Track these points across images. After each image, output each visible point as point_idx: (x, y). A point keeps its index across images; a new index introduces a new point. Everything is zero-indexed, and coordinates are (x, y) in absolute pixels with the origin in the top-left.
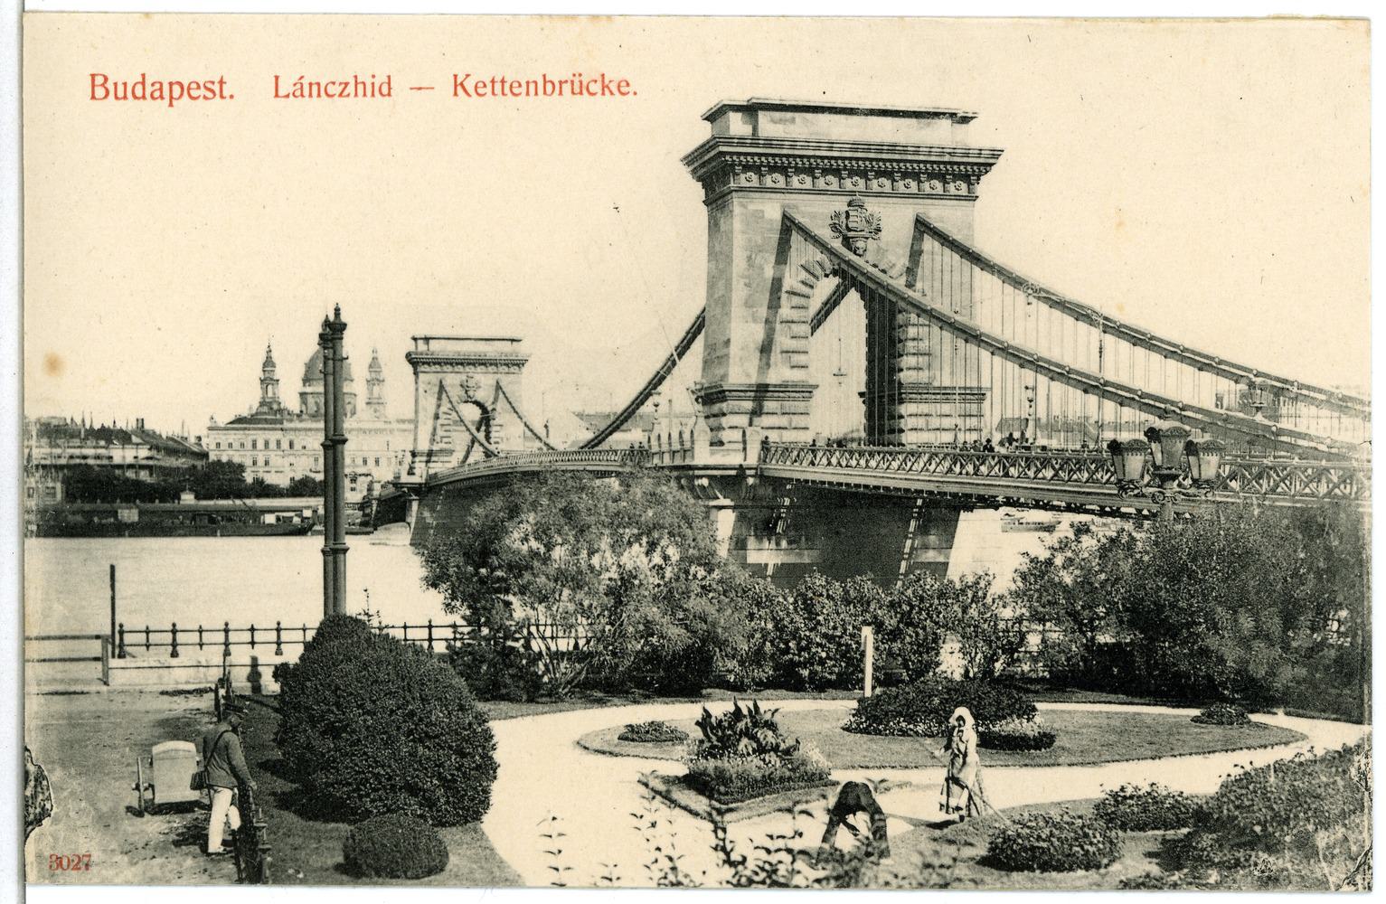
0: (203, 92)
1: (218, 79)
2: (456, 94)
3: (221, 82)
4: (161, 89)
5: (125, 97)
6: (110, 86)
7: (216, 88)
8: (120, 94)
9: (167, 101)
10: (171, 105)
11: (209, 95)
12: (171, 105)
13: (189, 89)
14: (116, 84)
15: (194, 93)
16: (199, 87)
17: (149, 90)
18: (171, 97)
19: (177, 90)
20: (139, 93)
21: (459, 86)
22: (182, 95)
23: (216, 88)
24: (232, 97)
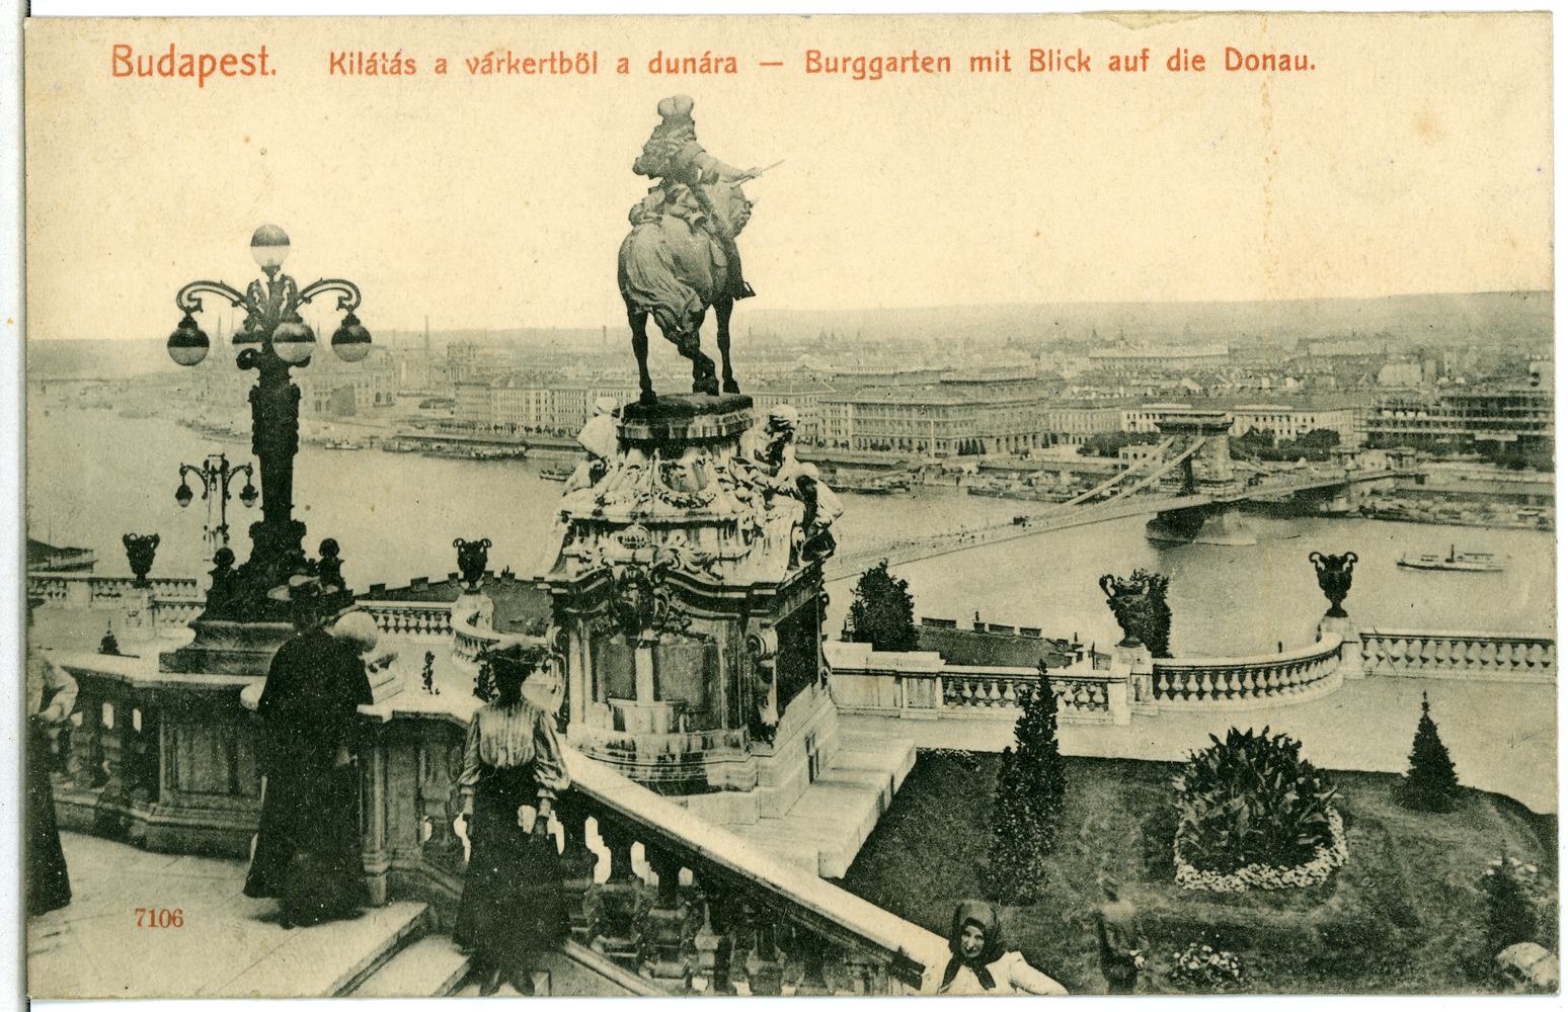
0: (240, 66)
1: (257, 52)
2: (332, 72)
3: (263, 56)
4: (191, 64)
5: (150, 73)
6: (134, 59)
7: (257, 62)
8: (145, 69)
9: (197, 76)
10: (201, 84)
11: (248, 69)
12: (201, 84)
13: (223, 62)
14: (140, 58)
15: (228, 68)
16: (235, 62)
17: (179, 62)
18: (202, 75)
19: (208, 64)
20: (166, 67)
21: (335, 63)
22: (213, 69)
23: (257, 62)
24: (274, 72)
